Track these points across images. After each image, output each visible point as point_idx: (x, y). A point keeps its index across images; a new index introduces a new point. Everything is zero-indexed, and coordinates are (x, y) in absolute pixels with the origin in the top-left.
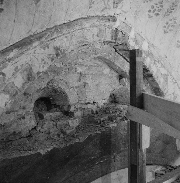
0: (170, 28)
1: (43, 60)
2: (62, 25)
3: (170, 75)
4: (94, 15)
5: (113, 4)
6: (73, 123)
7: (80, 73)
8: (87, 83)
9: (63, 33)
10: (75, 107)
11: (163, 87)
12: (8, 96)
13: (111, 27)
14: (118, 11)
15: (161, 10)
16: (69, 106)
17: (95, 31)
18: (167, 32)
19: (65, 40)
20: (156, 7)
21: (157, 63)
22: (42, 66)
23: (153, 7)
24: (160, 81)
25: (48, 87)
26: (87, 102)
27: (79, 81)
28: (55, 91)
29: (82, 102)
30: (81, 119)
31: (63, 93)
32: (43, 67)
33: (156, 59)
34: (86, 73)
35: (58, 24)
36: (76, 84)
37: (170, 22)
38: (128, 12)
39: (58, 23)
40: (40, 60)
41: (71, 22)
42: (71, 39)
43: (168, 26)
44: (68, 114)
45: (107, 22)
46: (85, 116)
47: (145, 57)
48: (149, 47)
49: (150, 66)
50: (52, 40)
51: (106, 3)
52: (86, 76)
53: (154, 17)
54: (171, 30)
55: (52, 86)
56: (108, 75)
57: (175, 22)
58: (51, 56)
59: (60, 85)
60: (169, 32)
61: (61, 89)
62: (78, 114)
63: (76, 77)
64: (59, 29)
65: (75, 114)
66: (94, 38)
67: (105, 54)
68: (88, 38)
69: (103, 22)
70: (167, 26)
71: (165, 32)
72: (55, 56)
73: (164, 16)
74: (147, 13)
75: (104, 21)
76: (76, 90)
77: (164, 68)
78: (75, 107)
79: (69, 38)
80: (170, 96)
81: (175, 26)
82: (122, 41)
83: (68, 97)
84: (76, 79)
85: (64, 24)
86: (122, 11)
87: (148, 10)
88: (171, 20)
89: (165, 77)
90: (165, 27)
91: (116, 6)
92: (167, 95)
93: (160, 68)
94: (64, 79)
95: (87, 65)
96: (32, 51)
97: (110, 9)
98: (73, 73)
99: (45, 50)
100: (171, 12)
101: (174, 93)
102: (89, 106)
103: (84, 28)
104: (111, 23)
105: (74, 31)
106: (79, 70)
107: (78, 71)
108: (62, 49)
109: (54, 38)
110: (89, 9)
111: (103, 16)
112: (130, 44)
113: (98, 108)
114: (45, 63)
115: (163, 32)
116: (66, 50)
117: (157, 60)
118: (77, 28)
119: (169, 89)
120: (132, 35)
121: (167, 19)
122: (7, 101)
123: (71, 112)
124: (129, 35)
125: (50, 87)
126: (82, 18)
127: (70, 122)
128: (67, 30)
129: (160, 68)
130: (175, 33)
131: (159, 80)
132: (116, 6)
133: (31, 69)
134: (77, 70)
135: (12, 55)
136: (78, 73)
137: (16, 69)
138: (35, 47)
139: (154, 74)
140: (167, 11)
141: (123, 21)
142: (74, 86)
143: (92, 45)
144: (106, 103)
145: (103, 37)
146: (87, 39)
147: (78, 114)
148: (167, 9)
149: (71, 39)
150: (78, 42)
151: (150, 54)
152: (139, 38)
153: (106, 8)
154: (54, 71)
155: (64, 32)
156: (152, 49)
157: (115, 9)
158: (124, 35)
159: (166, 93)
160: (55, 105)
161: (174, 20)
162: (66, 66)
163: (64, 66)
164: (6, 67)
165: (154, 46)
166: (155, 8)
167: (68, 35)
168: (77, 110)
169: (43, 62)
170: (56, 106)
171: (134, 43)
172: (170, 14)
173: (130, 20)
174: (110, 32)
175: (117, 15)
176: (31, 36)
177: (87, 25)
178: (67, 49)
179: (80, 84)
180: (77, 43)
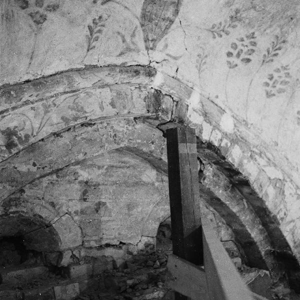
0: (278, 86)
2: (21, 84)
3: (288, 180)
4: (101, 64)
5: (145, 41)
6: (65, 291)
7: (87, 183)
8: (104, 204)
9: (24, 99)
10: (73, 256)
11: (275, 206)
13: (145, 87)
14: (157, 56)
15: (253, 51)
16: (60, 254)
17: (107, 95)
18: (274, 95)
19: (31, 114)
20: (243, 45)
21: (257, 157)
23: (234, 46)
24: (267, 195)
25: (6, 214)
26: (104, 242)
28: (28, 222)
29: (93, 244)
30: (86, 281)
31: (47, 227)
33: (254, 149)
34: (100, 180)
35: (12, 83)
36: (77, 206)
37: (276, 75)
38: (181, 57)
41: (43, 77)
42: (46, 112)
43: (274, 83)
44: (61, 273)
45: (133, 76)
46: (97, 275)
49: (241, 164)
51: (128, 39)
52: (101, 187)
54: (281, 91)
55: (17, 212)
56: (153, 184)
57: (288, 75)
59: (37, 210)
61: (41, 217)
62: (79, 270)
63: (75, 190)
64: (12, 93)
65: (72, 270)
66: (102, 108)
67: (140, 141)
68: (87, 110)
69: (125, 77)
70: (271, 83)
71: (269, 95)
72: (4, 148)
73: (262, 64)
74: (225, 58)
75: (126, 76)
76: (76, 218)
77: (275, 166)
78: (73, 256)
79: (41, 110)
80: (292, 224)
81: (289, 82)
82: (172, 114)
83: (57, 234)
84: (77, 195)
85: (28, 81)
86: (167, 55)
87: (224, 51)
88: (278, 70)
90: (267, 84)
91: (151, 46)
92: (284, 222)
94: (47, 197)
95: (103, 167)
97: (139, 51)
98: (70, 182)
100: (276, 55)
102: (109, 252)
103: (79, 90)
104: (143, 79)
105: (52, 97)
106: (84, 175)
107: (80, 179)
108: (22, 134)
110: (88, 50)
111: (123, 65)
112: (191, 119)
113: (130, 257)
115: (264, 95)
116: (32, 134)
117: (257, 151)
118: (61, 89)
119: (288, 209)
120: (194, 102)
121: (269, 69)
123: (63, 267)
124: (188, 102)
125: (11, 215)
126: (72, 70)
127: (58, 289)
128: (35, 94)
130: (290, 96)
131: (264, 192)
132: (151, 46)
134: (79, 176)
136: (80, 182)
139: (252, 179)
140: (267, 53)
141: (173, 74)
142: (71, 210)
143: (105, 125)
144: (150, 244)
145: (124, 107)
146: (86, 112)
147: (79, 270)
148: (266, 49)
149: (46, 112)
150: (62, 118)
151: (241, 139)
152: (211, 108)
153: (129, 49)
154: (13, 181)
155: (26, 97)
156: (242, 129)
157: (150, 51)
158: (177, 102)
159: (282, 219)
160: (33, 251)
161: (286, 71)
162: (43, 168)
163: (38, 168)
165: (246, 124)
166: (240, 47)
167: (40, 103)
168: (78, 264)
170: (36, 254)
171: (202, 118)
172: (275, 58)
173: (188, 74)
174: (143, 97)
175: (157, 63)
177: (81, 82)
178: (35, 134)
179: (85, 204)
180: (61, 121)
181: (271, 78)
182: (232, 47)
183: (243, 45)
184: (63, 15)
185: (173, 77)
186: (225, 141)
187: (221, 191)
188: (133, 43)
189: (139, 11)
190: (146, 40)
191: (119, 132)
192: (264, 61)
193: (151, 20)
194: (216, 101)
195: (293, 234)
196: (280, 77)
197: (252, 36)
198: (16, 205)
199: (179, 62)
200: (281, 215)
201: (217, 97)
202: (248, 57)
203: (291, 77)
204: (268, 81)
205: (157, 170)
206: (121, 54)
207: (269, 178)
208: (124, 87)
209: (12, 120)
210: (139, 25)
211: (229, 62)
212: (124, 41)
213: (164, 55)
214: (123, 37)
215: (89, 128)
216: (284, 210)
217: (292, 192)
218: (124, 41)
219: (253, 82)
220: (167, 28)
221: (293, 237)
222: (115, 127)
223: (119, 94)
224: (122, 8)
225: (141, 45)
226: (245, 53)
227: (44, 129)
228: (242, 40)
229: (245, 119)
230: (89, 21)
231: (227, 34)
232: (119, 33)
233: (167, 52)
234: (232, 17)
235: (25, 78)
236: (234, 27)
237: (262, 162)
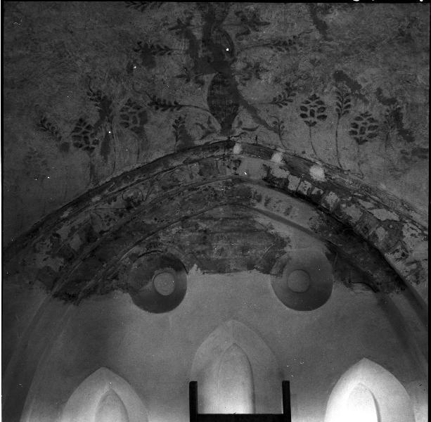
0: (367, 132)
1: (108, 216)
2: (135, 170)
7: (205, 231)
12: (62, 260)
15: (324, 108)
18: (367, 141)
19: (142, 188)
21: (360, 201)
22: (106, 223)
24: (375, 236)
27: (204, 244)
32: (108, 225)
37: (359, 123)
39: (128, 169)
40: (103, 216)
43: (361, 130)
48: (326, 174)
50: (120, 191)
51: (206, 126)
53: (320, 122)
54: (371, 136)
57: (372, 120)
58: (120, 210)
61: (172, 255)
66: (191, 177)
67: (239, 197)
70: (358, 130)
71: (360, 142)
73: (339, 117)
74: (301, 119)
75: (208, 152)
77: (387, 208)
80: (414, 266)
87: (297, 115)
88: (358, 119)
90: (353, 133)
93: (372, 209)
96: (92, 208)
99: (110, 204)
100: (349, 106)
105: (155, 175)
106: (203, 226)
107: (200, 228)
109: (123, 189)
114: (110, 220)
118: (160, 169)
119: (408, 249)
121: (347, 120)
122: (61, 265)
126: (167, 155)
129: (372, 209)
130: (385, 138)
133: (91, 228)
135: (66, 214)
136: (200, 231)
137: (73, 230)
138: (97, 202)
140: (338, 108)
145: (210, 174)
153: (209, 133)
161: (368, 118)
164: (60, 228)
165: (342, 171)
166: (309, 109)
169: (108, 219)
171: (288, 173)
176: (90, 191)
181: (356, 126)
182: (302, 109)
183: (311, 106)
184: (152, 124)
186: (316, 189)
187: (330, 235)
188: (211, 128)
189: (206, 106)
191: (219, 192)
192: (339, 114)
193: (219, 109)
194: (304, 156)
196: (366, 124)
197: (314, 97)
198: (155, 247)
199: (256, 132)
201: (304, 152)
202: (322, 114)
203: (377, 121)
205: (348, 223)
206: (203, 138)
207: (379, 220)
208: (210, 160)
209: (130, 193)
210: (211, 115)
211: (307, 122)
212: (203, 128)
213: (241, 129)
214: (201, 126)
215: (195, 192)
217: (414, 232)
218: (203, 128)
219: (338, 133)
222: (216, 189)
223: (206, 166)
224: (194, 109)
226: (318, 112)
227: (150, 196)
228: (307, 103)
229: (339, 166)
230: (172, 122)
231: (291, 101)
232: (197, 124)
234: (287, 89)
235: (137, 166)
236: (294, 95)
237: (368, 205)
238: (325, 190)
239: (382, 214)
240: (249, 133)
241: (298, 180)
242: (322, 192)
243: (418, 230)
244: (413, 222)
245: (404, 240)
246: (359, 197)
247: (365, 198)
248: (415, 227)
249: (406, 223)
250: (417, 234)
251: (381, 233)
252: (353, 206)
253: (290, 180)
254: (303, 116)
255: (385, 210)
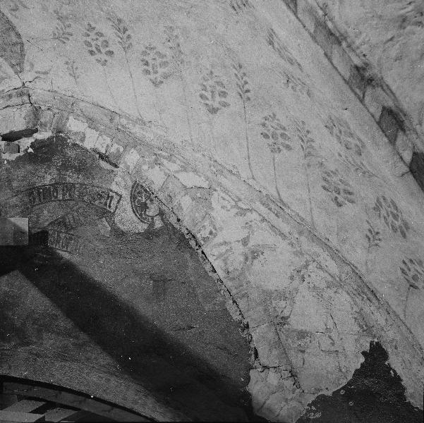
5: (12, 67)
14: (28, 76)
18: (162, 82)
21: (165, 162)
47: (122, 150)
54: (166, 76)
60: (164, 80)
77: (195, 171)
80: (223, 249)
89: (203, 197)
91: (19, 69)
93: (177, 172)
101: (245, 242)
119: (218, 226)
157: (20, 74)
174: (23, 116)
175: (30, 82)
185: (49, 91)
186: (116, 146)
190: (13, 66)
195: (225, 261)
200: (205, 233)
204: (146, 67)
207: (185, 187)
216: (209, 228)
220: (22, 50)
221: (226, 264)
225: (10, 71)
233: (35, 69)
234: (58, 19)
236: (69, 26)
237: (173, 167)
238: (125, 147)
239: (189, 179)
240: (42, 76)
241: (96, 134)
242: (122, 150)
243: (232, 201)
244: (226, 191)
245: (213, 214)
246: (164, 158)
247: (170, 158)
248: (227, 197)
249: (215, 190)
250: (229, 207)
251: (186, 202)
252: (157, 167)
253: (87, 136)
254: (92, 53)
255: (191, 174)
